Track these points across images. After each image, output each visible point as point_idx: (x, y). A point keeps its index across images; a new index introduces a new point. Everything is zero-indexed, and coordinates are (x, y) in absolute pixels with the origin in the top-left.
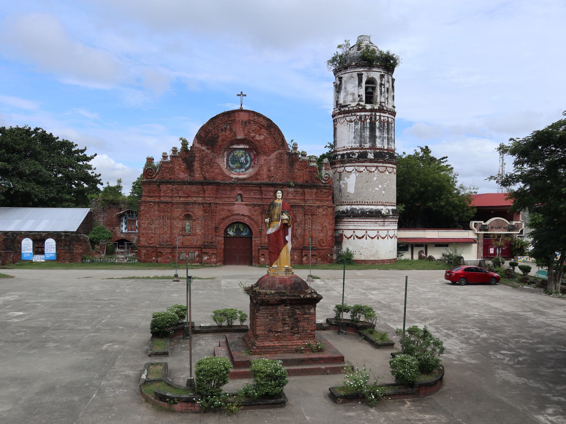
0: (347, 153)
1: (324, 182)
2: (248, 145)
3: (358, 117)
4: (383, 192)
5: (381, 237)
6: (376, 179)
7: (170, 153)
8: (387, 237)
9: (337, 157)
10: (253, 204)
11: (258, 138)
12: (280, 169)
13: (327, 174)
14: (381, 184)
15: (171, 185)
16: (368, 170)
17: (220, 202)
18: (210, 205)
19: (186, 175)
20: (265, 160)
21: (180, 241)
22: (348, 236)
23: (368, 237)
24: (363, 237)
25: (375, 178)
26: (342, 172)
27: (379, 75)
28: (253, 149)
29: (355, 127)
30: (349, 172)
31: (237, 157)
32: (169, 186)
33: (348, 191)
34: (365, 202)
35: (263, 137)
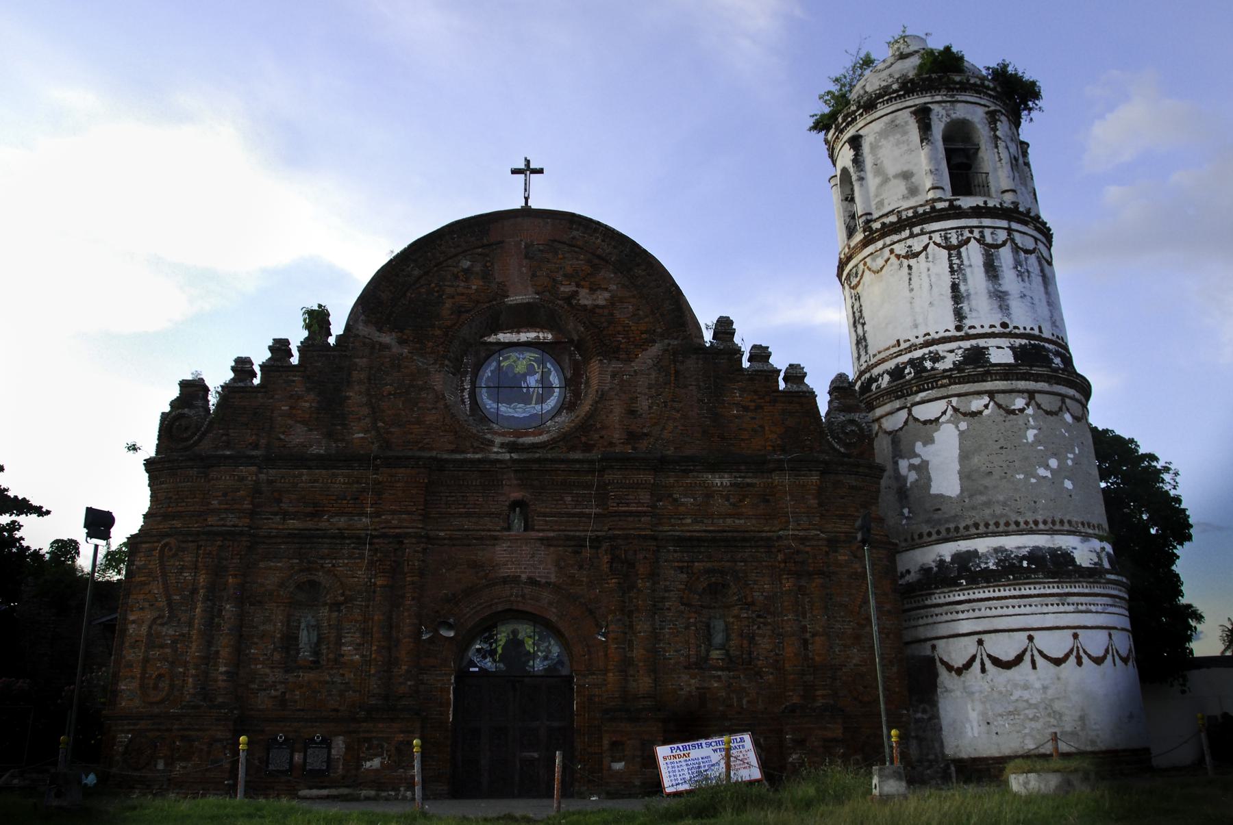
0: (911, 362)
1: (842, 450)
2: (551, 330)
3: (937, 238)
4: (1068, 484)
5: (1089, 656)
6: (1035, 436)
7: (260, 356)
8: (1109, 657)
9: (874, 386)
10: (573, 538)
11: (585, 298)
12: (675, 405)
13: (852, 422)
14: (1055, 455)
15: (254, 469)
16: (1000, 406)
17: (442, 534)
18: (402, 543)
19: (315, 435)
20: (614, 376)
22: (959, 662)
23: (1038, 659)
24: (1019, 659)
25: (1031, 434)
26: (901, 429)
27: (984, 115)
28: (571, 341)
29: (929, 270)
30: (931, 422)
31: (510, 375)
32: (243, 470)
33: (934, 491)
34: (1007, 524)
35: (607, 295)
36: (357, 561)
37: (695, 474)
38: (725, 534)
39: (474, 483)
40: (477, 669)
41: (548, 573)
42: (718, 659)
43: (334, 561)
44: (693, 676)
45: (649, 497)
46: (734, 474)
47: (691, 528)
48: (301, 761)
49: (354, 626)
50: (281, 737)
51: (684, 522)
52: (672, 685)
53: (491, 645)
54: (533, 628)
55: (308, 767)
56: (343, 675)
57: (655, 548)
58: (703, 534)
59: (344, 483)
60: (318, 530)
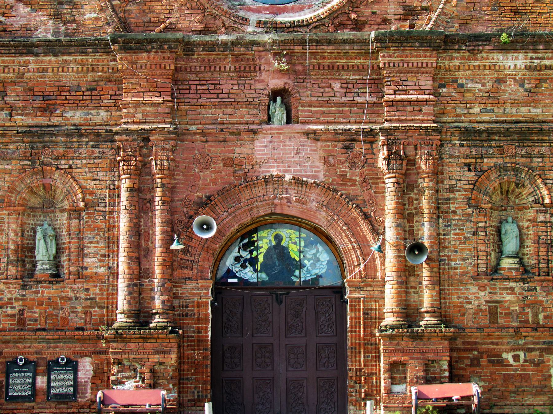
18: (147, 140)
21: (10, 311)
36: (97, 161)
37: (484, 55)
38: (519, 125)
39: (228, 69)
40: (235, 280)
41: (315, 172)
42: (509, 269)
43: (71, 162)
44: (482, 288)
45: (431, 83)
46: (530, 55)
47: (479, 119)
48: (45, 385)
49: (97, 234)
50: (21, 360)
51: (471, 111)
52: (459, 298)
53: (251, 252)
54: (298, 233)
55: (53, 392)
56: (87, 290)
57: (439, 143)
58: (494, 126)
59: (78, 72)
60: (49, 126)
